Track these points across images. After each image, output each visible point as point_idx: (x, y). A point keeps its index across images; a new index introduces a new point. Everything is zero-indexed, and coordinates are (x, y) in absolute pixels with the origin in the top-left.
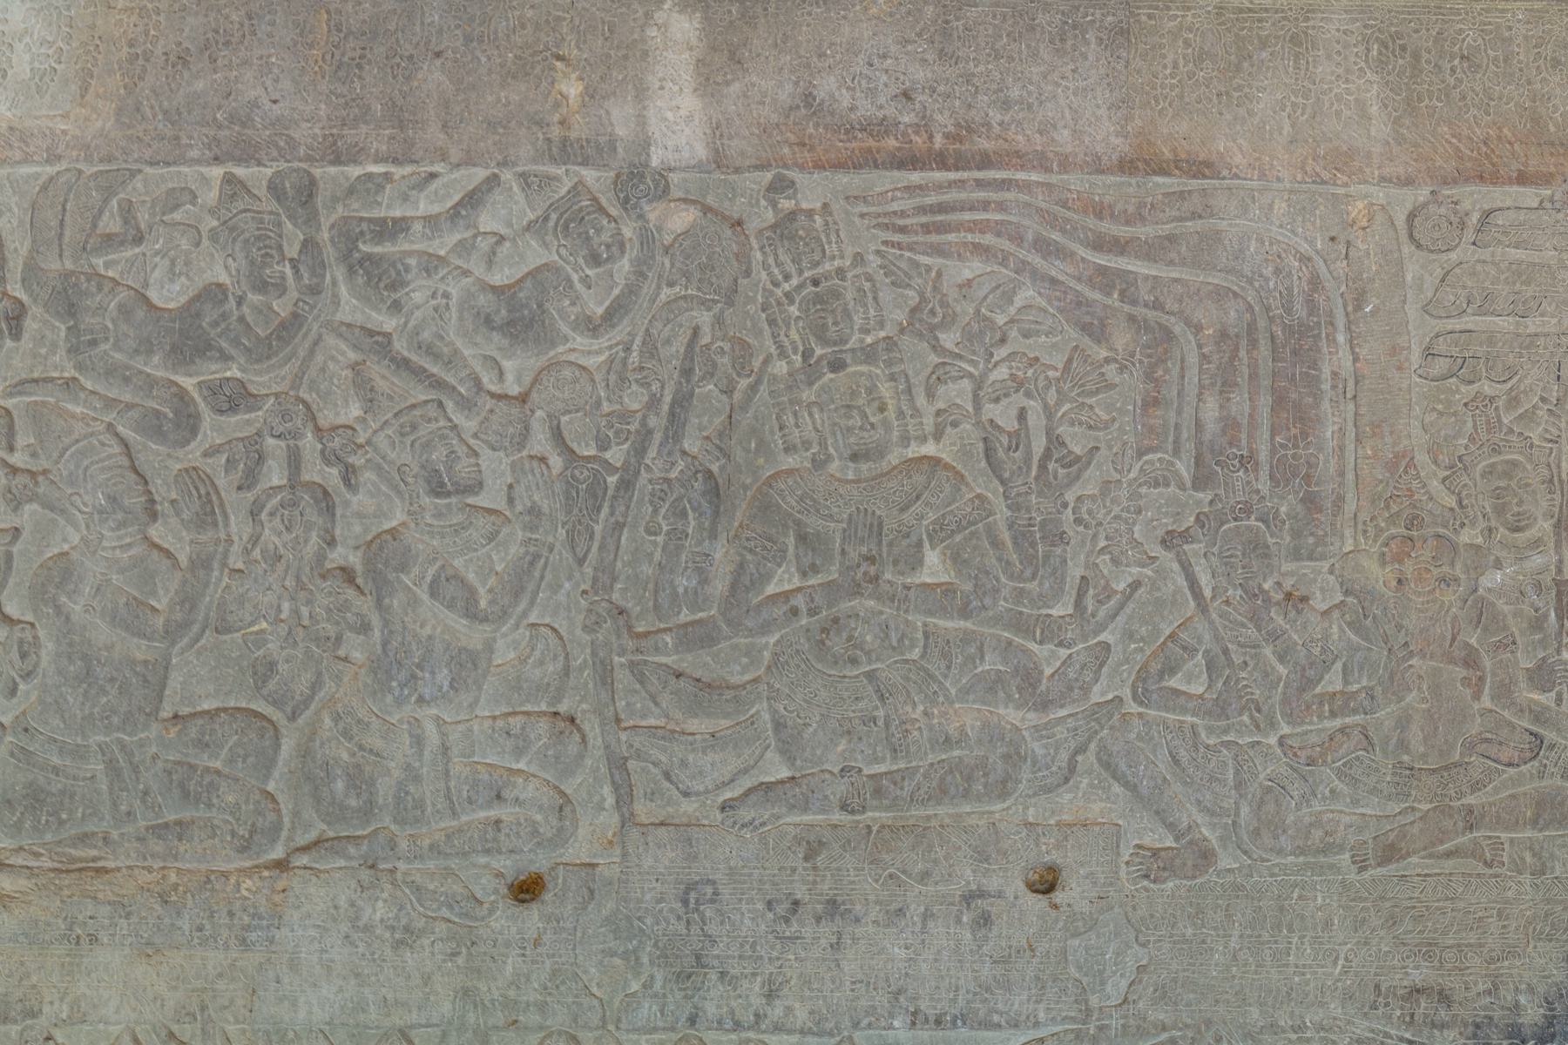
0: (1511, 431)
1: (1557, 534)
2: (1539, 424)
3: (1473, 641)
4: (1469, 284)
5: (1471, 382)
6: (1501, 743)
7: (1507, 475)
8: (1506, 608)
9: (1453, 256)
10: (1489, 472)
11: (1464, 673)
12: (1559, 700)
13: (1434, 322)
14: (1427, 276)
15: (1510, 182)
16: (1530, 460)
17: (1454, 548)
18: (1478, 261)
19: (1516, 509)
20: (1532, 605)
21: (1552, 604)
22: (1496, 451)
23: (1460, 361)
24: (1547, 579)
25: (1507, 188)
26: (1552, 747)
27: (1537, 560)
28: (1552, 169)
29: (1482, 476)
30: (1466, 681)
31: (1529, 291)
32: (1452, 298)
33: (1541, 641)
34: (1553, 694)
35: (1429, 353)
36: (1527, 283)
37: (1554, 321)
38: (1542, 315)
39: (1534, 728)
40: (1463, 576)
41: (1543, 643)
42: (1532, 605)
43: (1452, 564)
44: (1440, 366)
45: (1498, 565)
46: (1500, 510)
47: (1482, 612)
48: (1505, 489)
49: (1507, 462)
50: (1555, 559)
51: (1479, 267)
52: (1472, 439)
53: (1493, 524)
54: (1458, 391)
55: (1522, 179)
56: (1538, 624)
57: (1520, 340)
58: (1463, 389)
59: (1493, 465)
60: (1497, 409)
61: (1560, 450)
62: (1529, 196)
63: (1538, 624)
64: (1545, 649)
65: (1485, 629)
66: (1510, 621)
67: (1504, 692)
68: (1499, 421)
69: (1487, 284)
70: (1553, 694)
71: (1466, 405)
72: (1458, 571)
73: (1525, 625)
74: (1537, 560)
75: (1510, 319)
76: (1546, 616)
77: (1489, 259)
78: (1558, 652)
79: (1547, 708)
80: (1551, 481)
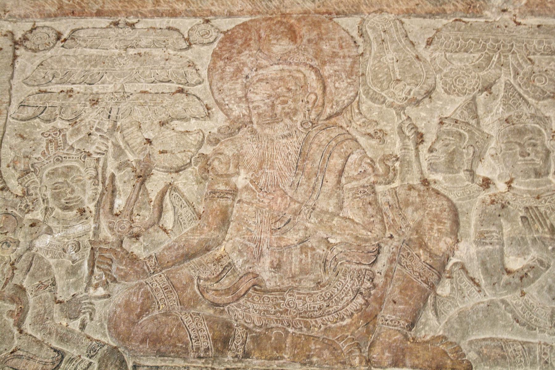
0: (72, 148)
1: (98, 211)
2: (93, 144)
3: (25, 285)
4: (56, 67)
5: (48, 121)
6: (29, 359)
7: (66, 175)
8: (52, 262)
9: (49, 54)
10: (53, 173)
11: (13, 307)
12: (83, 326)
13: (28, 88)
14: (29, 64)
15: (91, 15)
16: (84, 166)
17: (18, 221)
18: (64, 55)
19: (69, 196)
20: (70, 258)
21: (87, 257)
22: (59, 160)
23: (42, 109)
24: (85, 241)
25: (89, 19)
26: (71, 360)
27: (79, 228)
28: (120, 8)
29: (47, 176)
30: (11, 313)
31: (96, 70)
32: (43, 75)
33: (74, 283)
34: (78, 322)
35: (22, 105)
36: (95, 66)
37: (111, 86)
38: (103, 83)
39: (59, 347)
40: (22, 240)
41: (76, 286)
42: (70, 258)
43: (14, 231)
44: (29, 112)
45: (49, 231)
46: (56, 196)
47: (33, 263)
48: (62, 183)
49: (65, 167)
50: (93, 226)
51: (64, 58)
52: (44, 154)
53: (50, 205)
54: (39, 127)
55: (99, 14)
56: (73, 271)
57: (86, 96)
58: (43, 125)
59: (56, 169)
60: (64, 135)
61: (106, 159)
62: (104, 22)
63: (73, 271)
64: (76, 288)
65: (33, 275)
66: (54, 269)
67: (41, 320)
68: (65, 142)
69: (68, 67)
70: (78, 322)
71: (42, 134)
72: (20, 236)
73: (63, 272)
74: (79, 228)
75: (82, 86)
76: (80, 266)
77: (71, 54)
78: (86, 290)
79: (73, 331)
80: (96, 177)
